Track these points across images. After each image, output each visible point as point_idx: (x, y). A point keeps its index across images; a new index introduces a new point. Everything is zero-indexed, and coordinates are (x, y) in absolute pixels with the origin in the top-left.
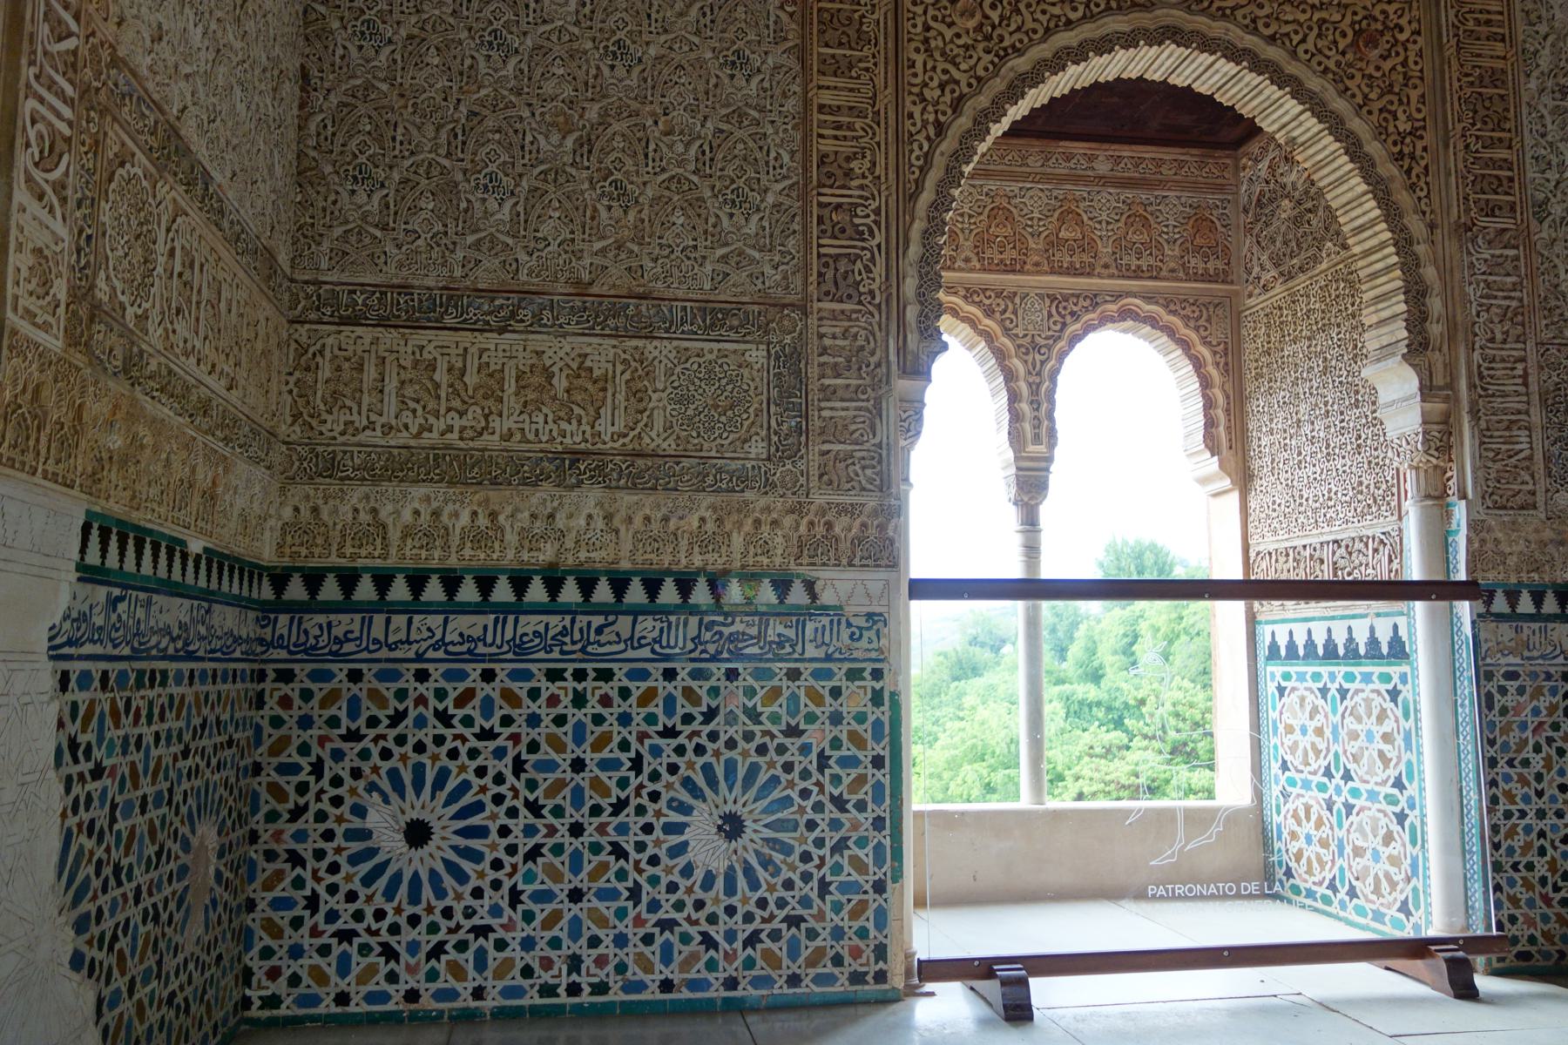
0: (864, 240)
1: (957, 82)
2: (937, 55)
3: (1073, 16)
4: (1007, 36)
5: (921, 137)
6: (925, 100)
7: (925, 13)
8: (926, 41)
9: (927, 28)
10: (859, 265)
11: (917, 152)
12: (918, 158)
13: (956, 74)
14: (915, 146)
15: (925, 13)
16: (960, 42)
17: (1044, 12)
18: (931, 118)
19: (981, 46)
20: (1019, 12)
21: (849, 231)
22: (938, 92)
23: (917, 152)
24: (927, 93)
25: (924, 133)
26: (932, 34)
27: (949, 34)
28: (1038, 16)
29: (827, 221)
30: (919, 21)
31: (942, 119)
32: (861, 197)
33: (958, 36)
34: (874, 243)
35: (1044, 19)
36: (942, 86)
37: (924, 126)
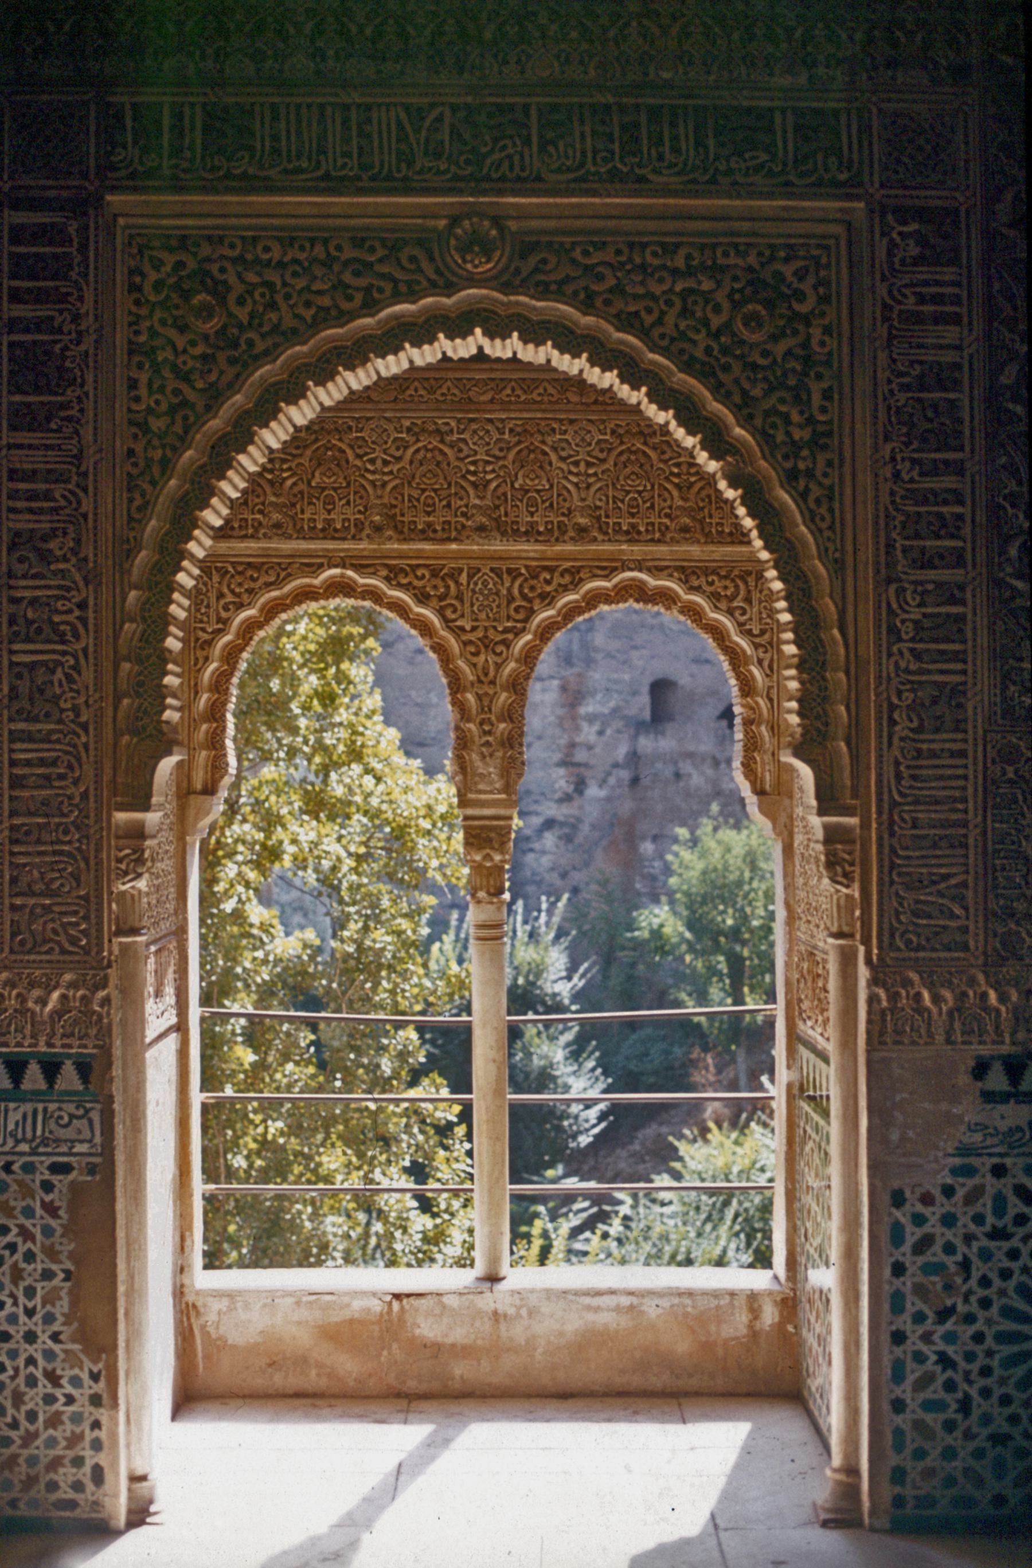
0: (63, 642)
2: (167, 373)
3: (346, 306)
10: (59, 674)
17: (308, 304)
21: (47, 630)
26: (157, 342)
28: (301, 310)
29: (21, 621)
32: (60, 587)
33: (193, 343)
34: (79, 646)
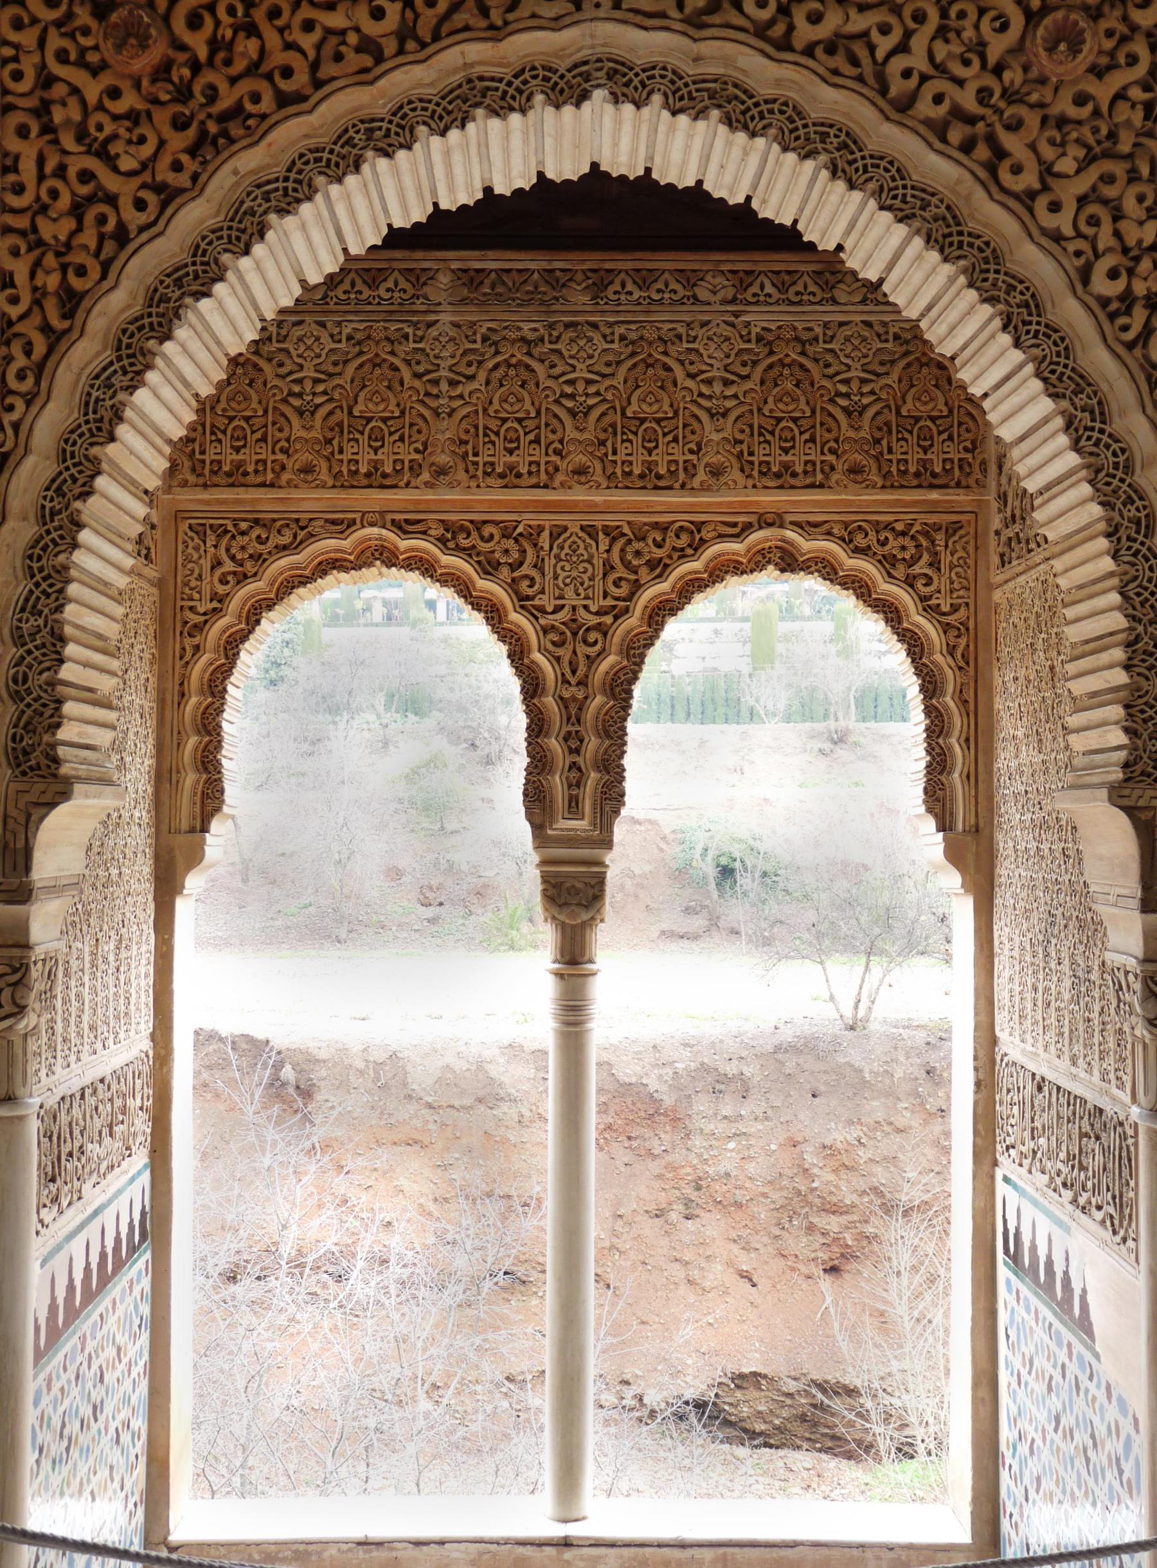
1: (112, 200)
4: (223, 86)
5: (29, 328)
6: (40, 243)
7: (42, 43)
8: (43, 110)
9: (47, 80)
11: (21, 361)
12: (21, 376)
13: (111, 182)
14: (16, 349)
15: (42, 43)
16: (120, 107)
18: (53, 282)
19: (162, 117)
20: (252, 30)
22: (69, 224)
23: (21, 361)
24: (46, 230)
25: (36, 319)
27: (93, 90)
30: (28, 64)
31: (76, 283)
35: (308, 42)
36: (77, 210)
37: (37, 303)
